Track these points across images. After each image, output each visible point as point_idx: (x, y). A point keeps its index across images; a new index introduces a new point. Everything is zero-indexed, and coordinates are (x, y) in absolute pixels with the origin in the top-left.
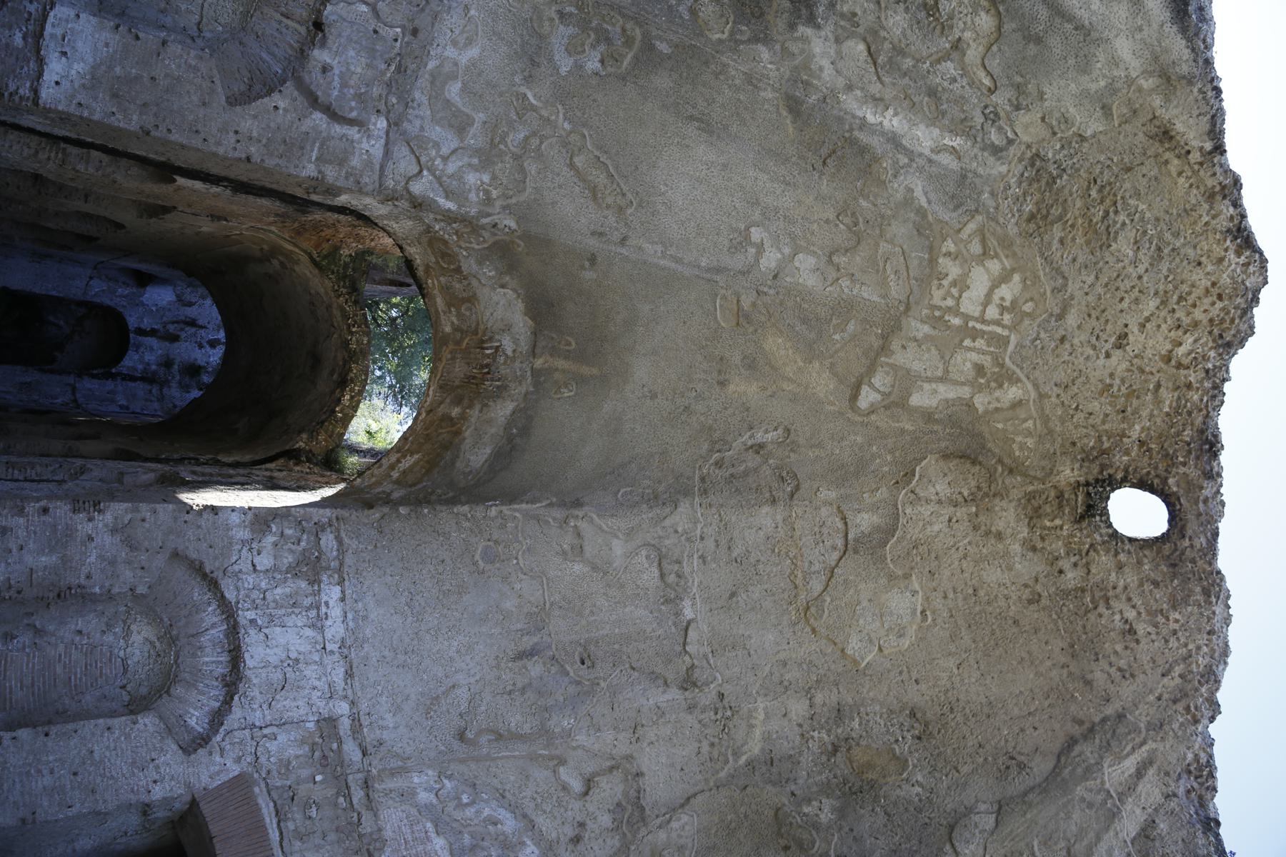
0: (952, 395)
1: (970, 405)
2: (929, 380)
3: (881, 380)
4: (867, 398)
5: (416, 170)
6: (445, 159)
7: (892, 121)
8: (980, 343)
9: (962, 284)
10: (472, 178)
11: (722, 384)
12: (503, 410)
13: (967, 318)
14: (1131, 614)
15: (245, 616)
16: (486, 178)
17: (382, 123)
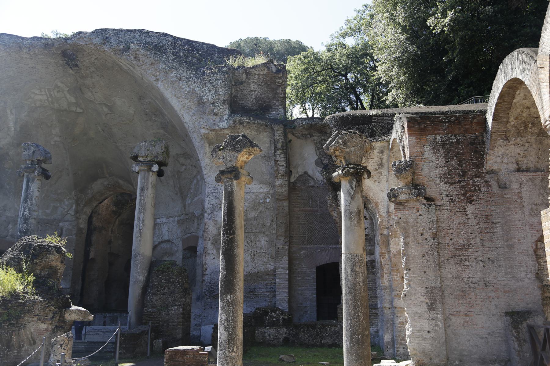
0: (68, 95)
1: (68, 91)
2: (67, 100)
3: (73, 109)
4: (79, 110)
5: (69, 215)
6: (64, 209)
7: (11, 125)
8: (52, 93)
9: (41, 100)
10: (67, 203)
11: (93, 138)
12: (121, 182)
13: (48, 97)
14: (93, 59)
15: (160, 239)
16: (65, 200)
17: (61, 224)
